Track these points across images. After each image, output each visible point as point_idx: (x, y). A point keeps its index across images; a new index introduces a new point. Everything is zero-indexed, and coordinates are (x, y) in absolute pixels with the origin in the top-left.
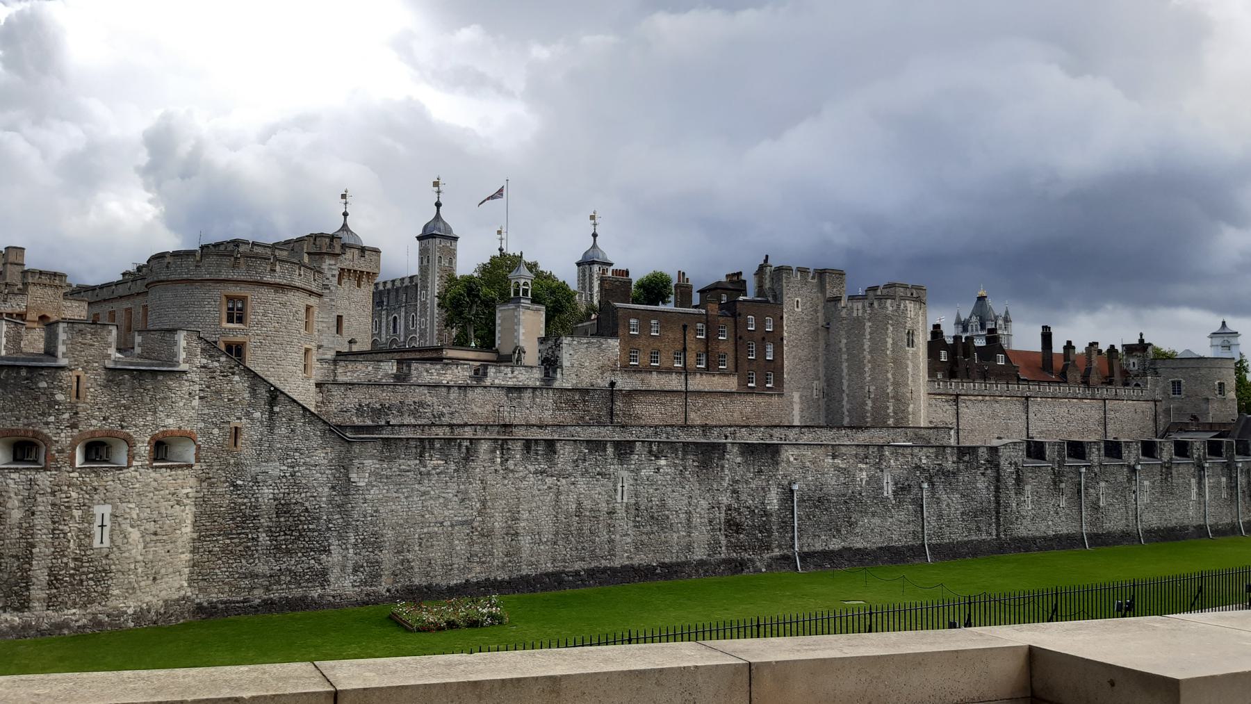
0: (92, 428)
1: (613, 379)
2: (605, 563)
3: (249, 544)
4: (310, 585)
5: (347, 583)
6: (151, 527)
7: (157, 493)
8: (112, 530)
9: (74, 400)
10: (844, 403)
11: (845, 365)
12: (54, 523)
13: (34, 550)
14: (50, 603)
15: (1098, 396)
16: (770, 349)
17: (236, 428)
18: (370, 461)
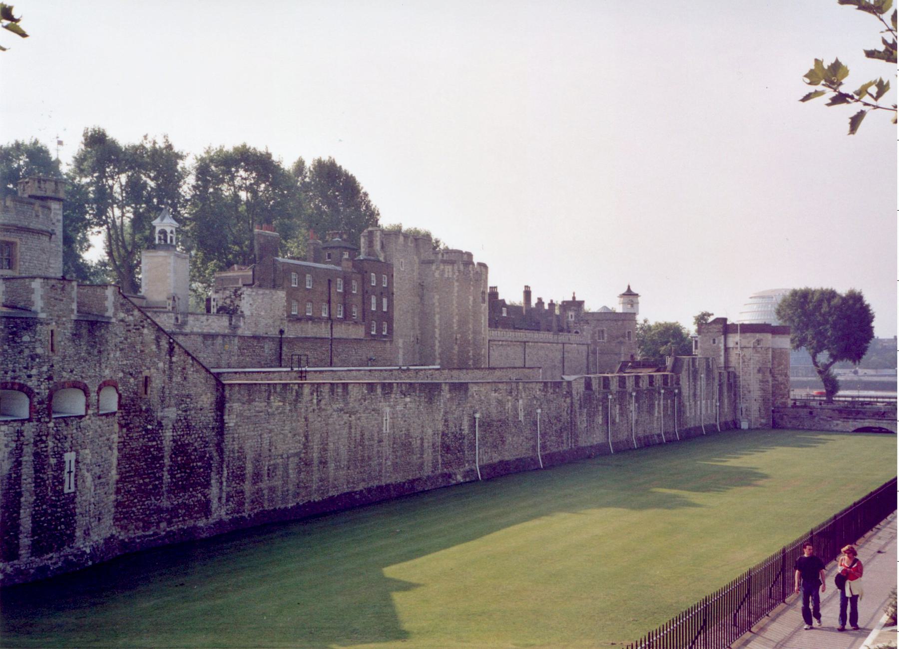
0: (63, 380)
1: (281, 327)
2: (376, 483)
3: (157, 483)
4: (198, 516)
5: (223, 513)
6: (97, 470)
7: (100, 439)
8: (76, 476)
9: (51, 354)
10: (437, 347)
11: (437, 316)
12: (36, 471)
13: (23, 499)
14: (37, 549)
15: (560, 341)
16: (385, 301)
17: (146, 377)
18: (236, 404)
